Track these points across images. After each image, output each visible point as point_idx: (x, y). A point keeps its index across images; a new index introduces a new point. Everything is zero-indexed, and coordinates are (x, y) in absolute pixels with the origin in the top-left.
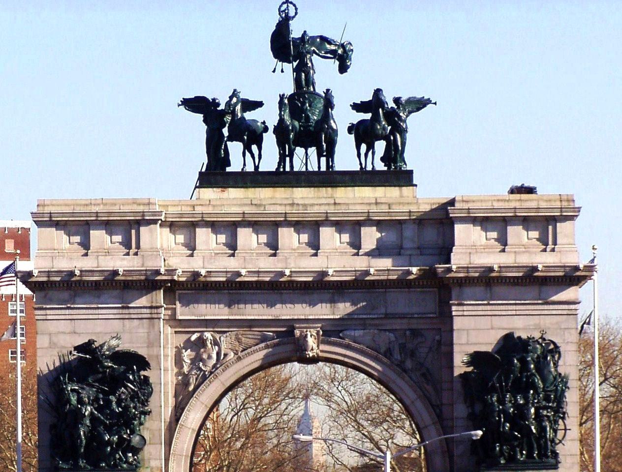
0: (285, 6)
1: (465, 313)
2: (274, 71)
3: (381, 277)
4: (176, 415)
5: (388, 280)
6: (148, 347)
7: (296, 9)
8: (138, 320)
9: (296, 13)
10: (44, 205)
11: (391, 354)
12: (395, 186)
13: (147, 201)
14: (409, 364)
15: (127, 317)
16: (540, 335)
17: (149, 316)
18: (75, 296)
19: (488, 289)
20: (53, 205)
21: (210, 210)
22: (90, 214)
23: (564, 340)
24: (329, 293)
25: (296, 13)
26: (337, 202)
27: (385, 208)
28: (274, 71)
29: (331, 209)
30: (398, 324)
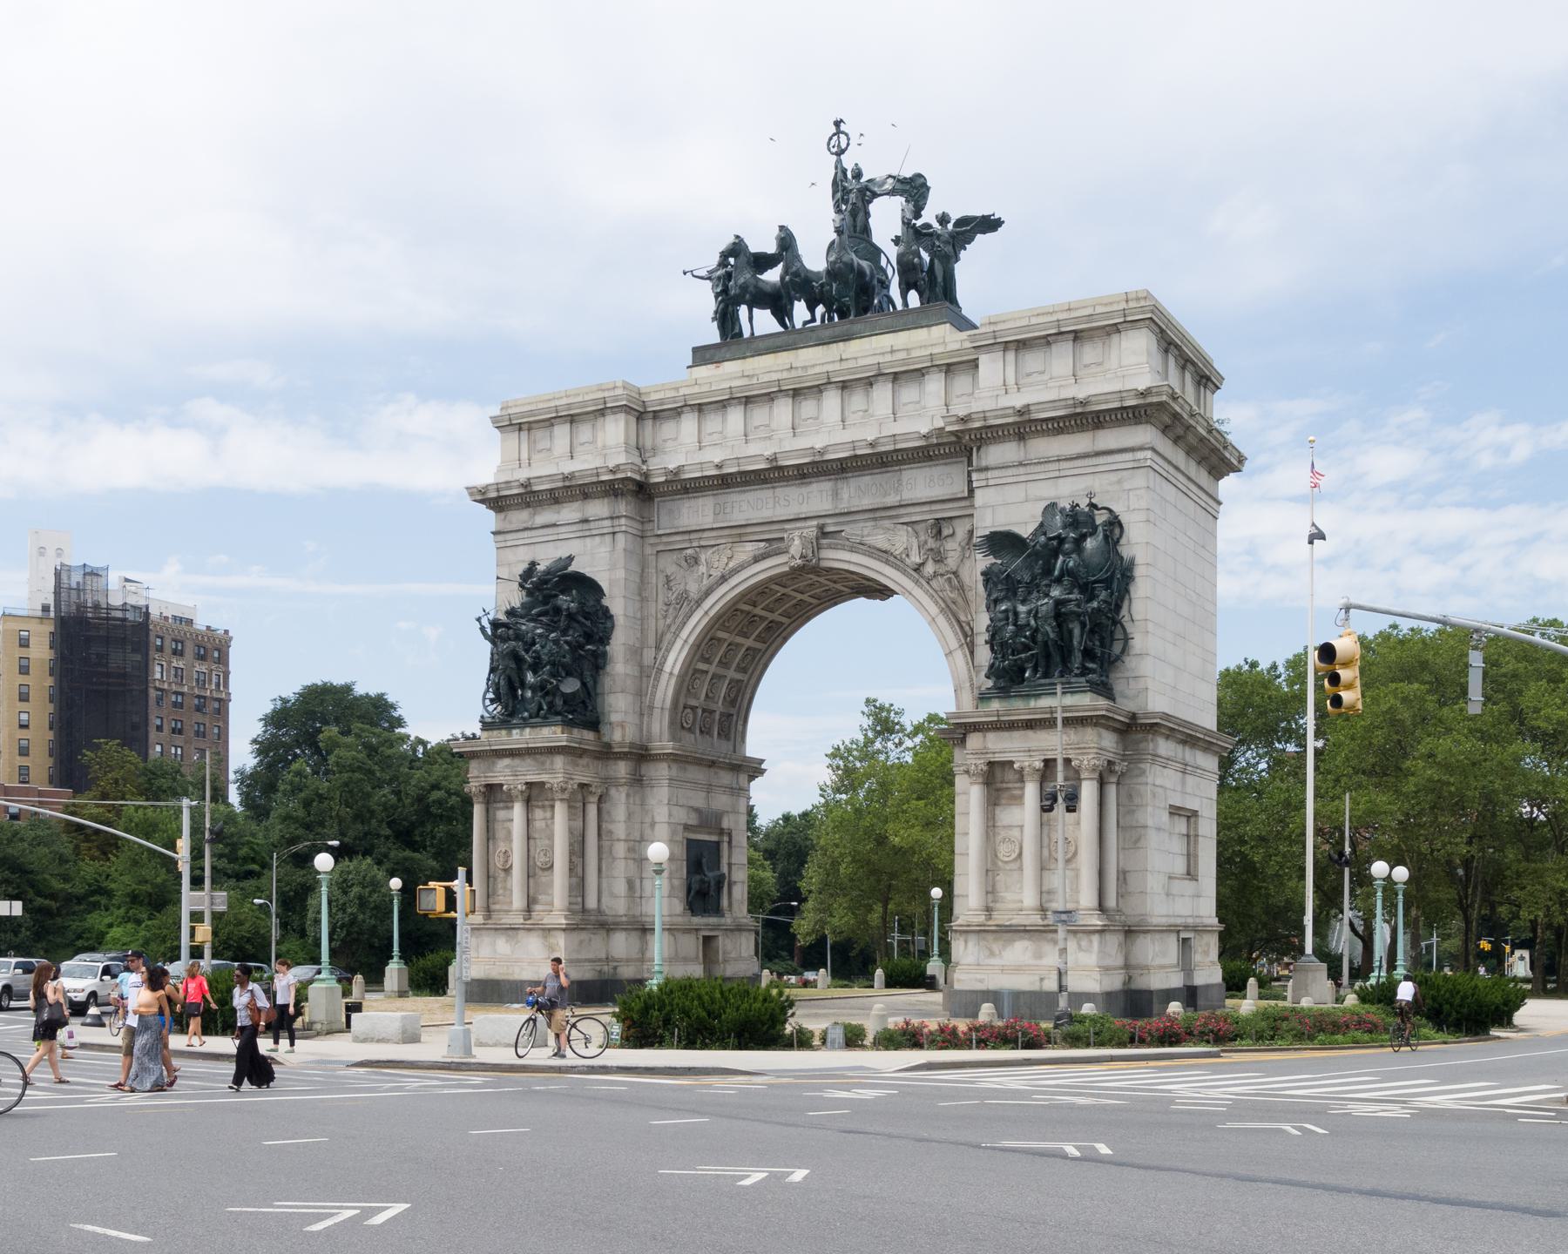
0: (835, 138)
1: (991, 482)
5: (896, 451)
7: (848, 139)
9: (848, 145)
10: (507, 407)
11: (908, 555)
12: (922, 327)
13: (611, 386)
16: (1087, 501)
17: (611, 530)
18: (534, 514)
19: (1022, 444)
20: (516, 406)
21: (696, 390)
22: (548, 410)
23: (1129, 507)
24: (830, 480)
25: (848, 145)
26: (843, 357)
27: (902, 355)
29: (837, 367)
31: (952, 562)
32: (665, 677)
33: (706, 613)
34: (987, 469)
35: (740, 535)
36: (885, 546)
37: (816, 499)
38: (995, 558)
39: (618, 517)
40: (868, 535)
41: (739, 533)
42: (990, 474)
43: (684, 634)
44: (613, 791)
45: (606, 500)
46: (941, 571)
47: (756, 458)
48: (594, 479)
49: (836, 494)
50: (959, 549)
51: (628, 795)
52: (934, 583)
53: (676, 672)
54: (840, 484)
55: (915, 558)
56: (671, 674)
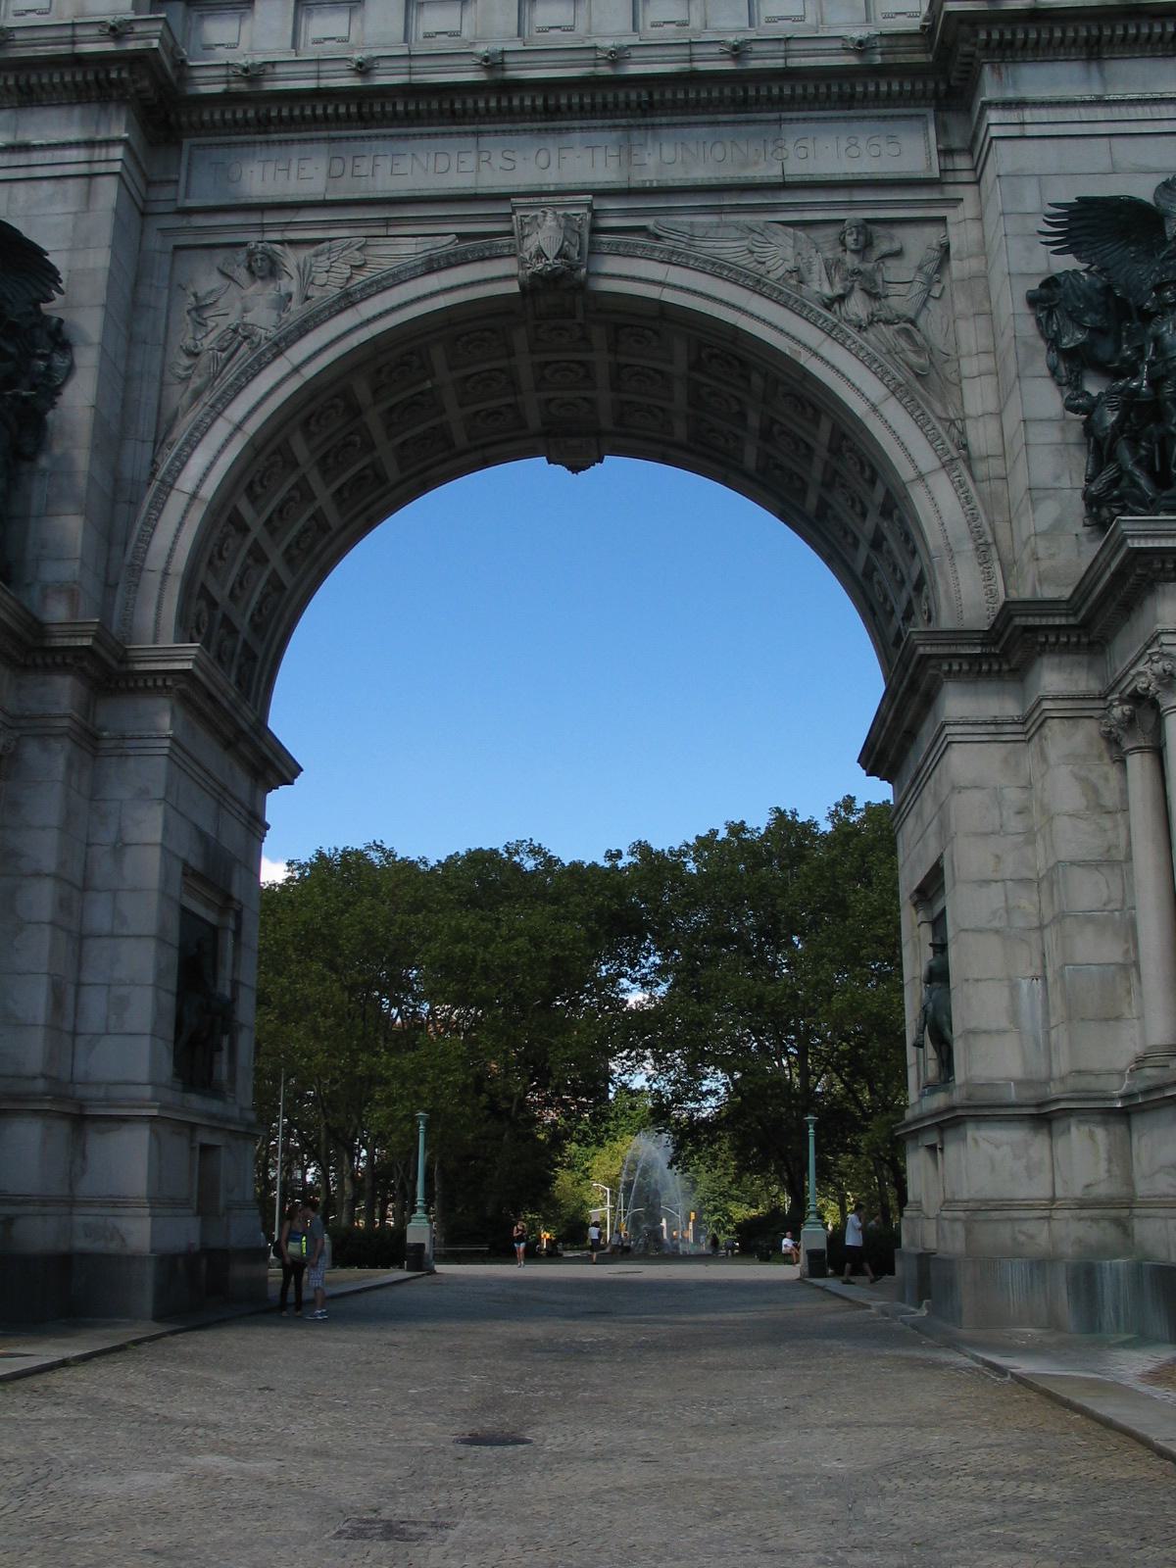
1: (1031, 130)
3: (768, 61)
4: (153, 462)
6: (70, 250)
8: (52, 182)
14: (857, 306)
15: (21, 176)
17: (83, 169)
24: (615, 127)
31: (900, 301)
32: (176, 504)
33: (296, 370)
36: (746, 261)
38: (1079, 258)
39: (108, 143)
40: (704, 238)
43: (237, 410)
44: (32, 751)
45: (77, 112)
46: (883, 314)
47: (457, 61)
50: (920, 278)
51: (70, 765)
52: (870, 335)
53: (208, 491)
55: (821, 286)
56: (194, 496)
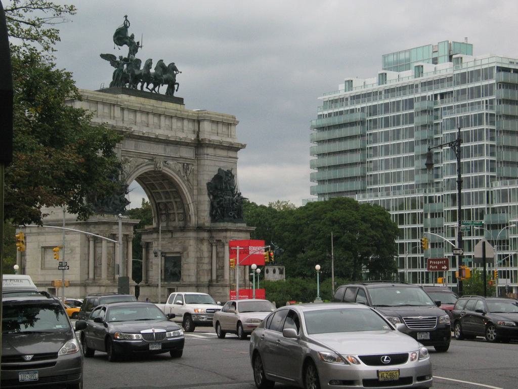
2: (115, 48)
7: (129, 24)
28: (115, 48)
30: (182, 161)
34: (208, 155)
35: (140, 155)
37: (158, 150)
41: (140, 155)
42: (209, 156)
48: (120, 130)
49: (165, 150)
54: (166, 147)
